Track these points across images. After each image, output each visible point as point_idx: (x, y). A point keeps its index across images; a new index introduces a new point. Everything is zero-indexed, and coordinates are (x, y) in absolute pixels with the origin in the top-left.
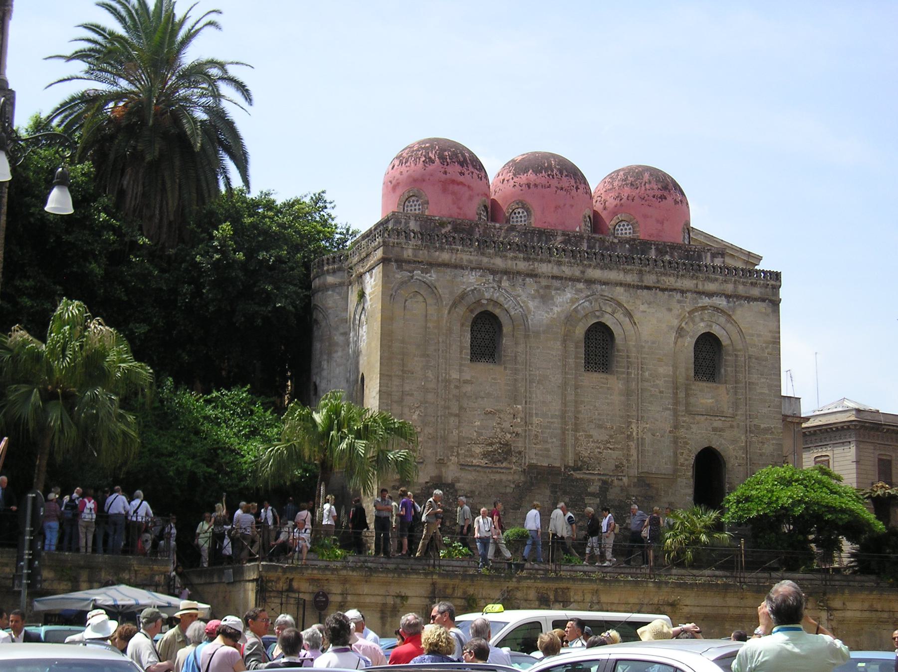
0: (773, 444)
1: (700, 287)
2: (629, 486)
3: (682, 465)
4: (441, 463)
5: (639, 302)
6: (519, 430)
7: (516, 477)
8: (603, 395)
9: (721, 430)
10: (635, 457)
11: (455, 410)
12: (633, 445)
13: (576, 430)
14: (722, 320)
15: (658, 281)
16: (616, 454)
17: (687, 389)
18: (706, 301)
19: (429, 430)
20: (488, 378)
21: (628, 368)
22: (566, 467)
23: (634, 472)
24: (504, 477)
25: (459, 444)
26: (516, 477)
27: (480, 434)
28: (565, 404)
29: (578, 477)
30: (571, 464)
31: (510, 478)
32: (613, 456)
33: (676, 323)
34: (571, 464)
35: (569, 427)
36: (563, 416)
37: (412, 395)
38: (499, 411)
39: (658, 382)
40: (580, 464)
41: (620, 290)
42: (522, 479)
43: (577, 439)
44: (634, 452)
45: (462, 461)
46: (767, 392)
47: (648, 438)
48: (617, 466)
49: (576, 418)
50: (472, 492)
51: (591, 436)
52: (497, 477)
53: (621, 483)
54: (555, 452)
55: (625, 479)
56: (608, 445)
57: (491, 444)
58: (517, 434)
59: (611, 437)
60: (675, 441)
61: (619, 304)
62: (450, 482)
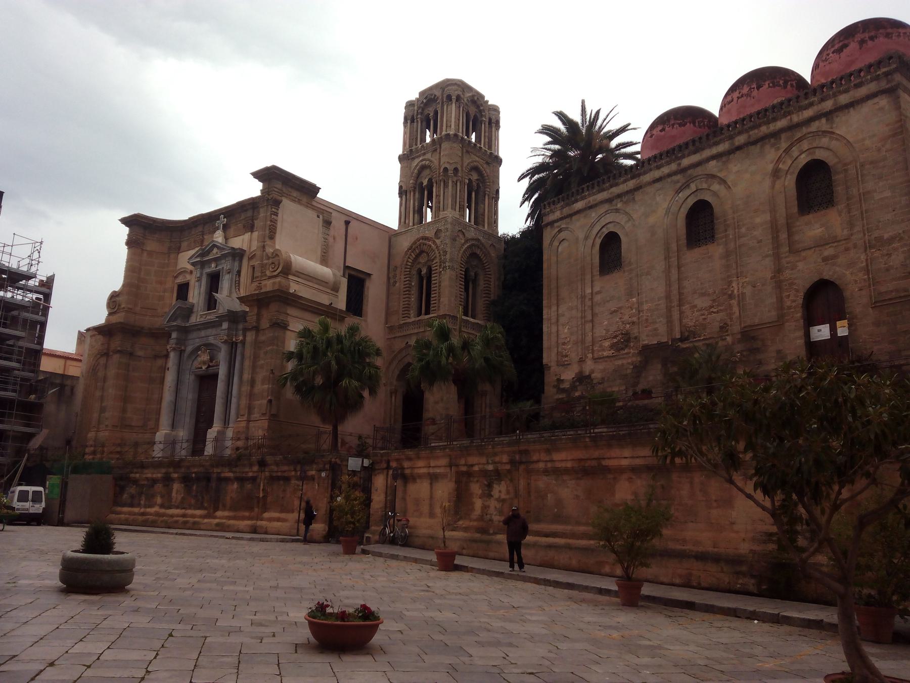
0: (903, 252)
1: (796, 118)
2: (733, 343)
3: (789, 308)
4: (581, 361)
5: (731, 166)
6: (635, 319)
7: (634, 359)
8: (705, 266)
9: (835, 257)
10: (737, 314)
11: (589, 317)
12: (734, 302)
13: (681, 304)
14: (825, 141)
15: (749, 136)
16: (718, 317)
17: (789, 227)
18: (804, 130)
19: (574, 338)
20: (615, 284)
21: (726, 231)
22: (673, 340)
23: (736, 328)
24: (625, 362)
25: (593, 343)
26: (634, 359)
27: (607, 331)
28: (669, 285)
29: (685, 346)
30: (678, 336)
31: (630, 361)
32: (716, 319)
33: (770, 167)
34: (678, 336)
35: (675, 303)
36: (668, 297)
37: (563, 315)
38: (620, 308)
39: (755, 233)
40: (687, 334)
41: (713, 163)
42: (639, 359)
43: (681, 313)
44: (736, 309)
45: (596, 356)
46: (890, 194)
47: (748, 291)
48: (721, 328)
49: (680, 294)
50: (603, 379)
51: (695, 306)
52: (620, 362)
53: (724, 343)
54: (662, 329)
55: (729, 339)
56: (713, 310)
57: (615, 337)
58: (633, 323)
59: (714, 301)
60: (779, 285)
61: (713, 176)
62: (587, 374)
